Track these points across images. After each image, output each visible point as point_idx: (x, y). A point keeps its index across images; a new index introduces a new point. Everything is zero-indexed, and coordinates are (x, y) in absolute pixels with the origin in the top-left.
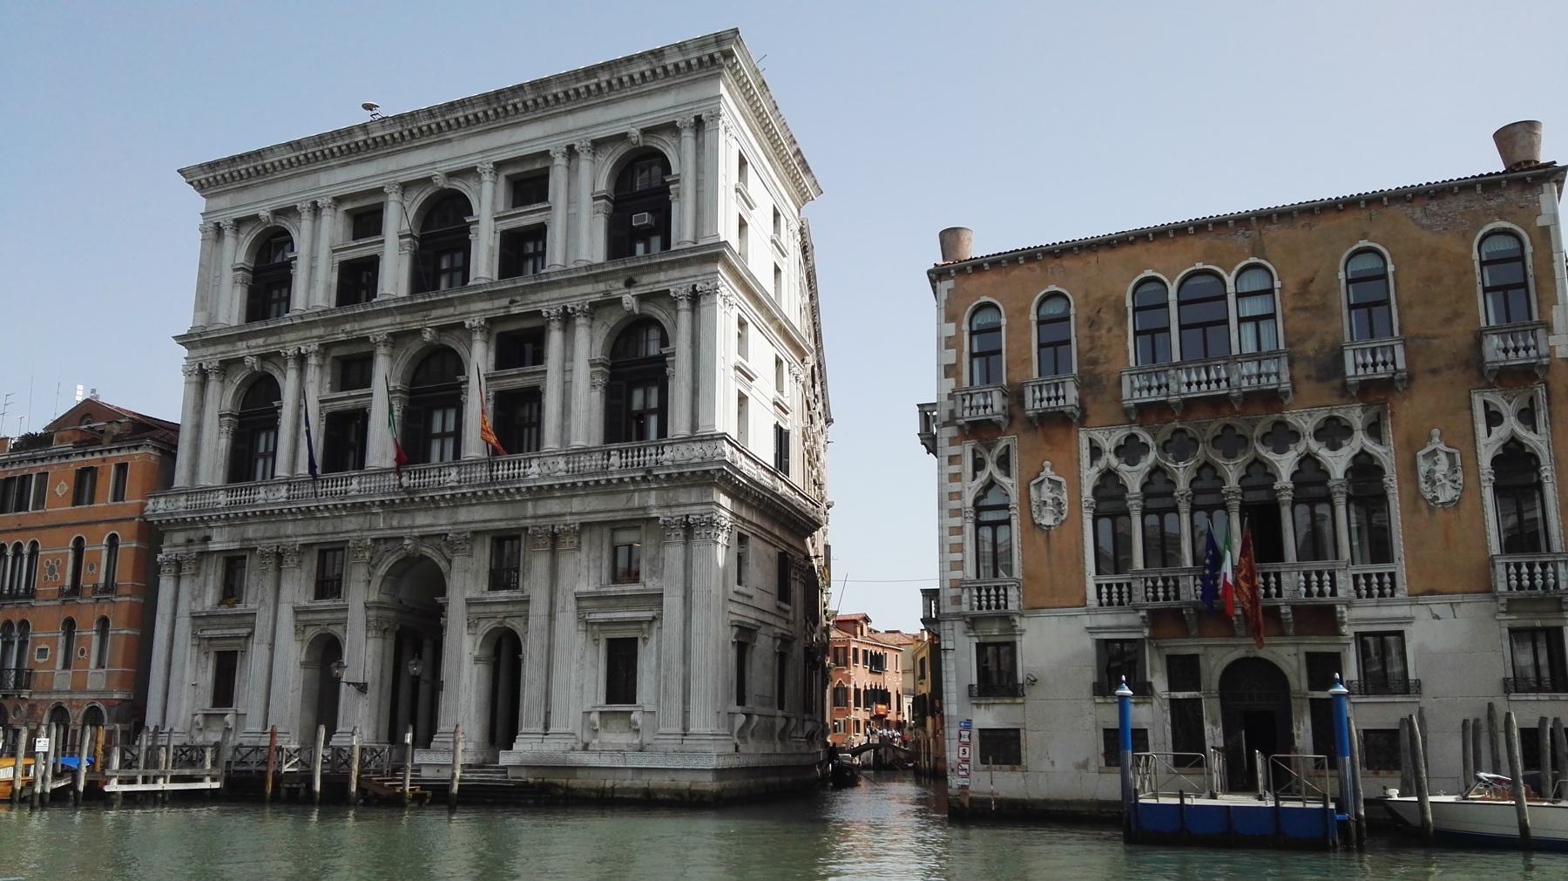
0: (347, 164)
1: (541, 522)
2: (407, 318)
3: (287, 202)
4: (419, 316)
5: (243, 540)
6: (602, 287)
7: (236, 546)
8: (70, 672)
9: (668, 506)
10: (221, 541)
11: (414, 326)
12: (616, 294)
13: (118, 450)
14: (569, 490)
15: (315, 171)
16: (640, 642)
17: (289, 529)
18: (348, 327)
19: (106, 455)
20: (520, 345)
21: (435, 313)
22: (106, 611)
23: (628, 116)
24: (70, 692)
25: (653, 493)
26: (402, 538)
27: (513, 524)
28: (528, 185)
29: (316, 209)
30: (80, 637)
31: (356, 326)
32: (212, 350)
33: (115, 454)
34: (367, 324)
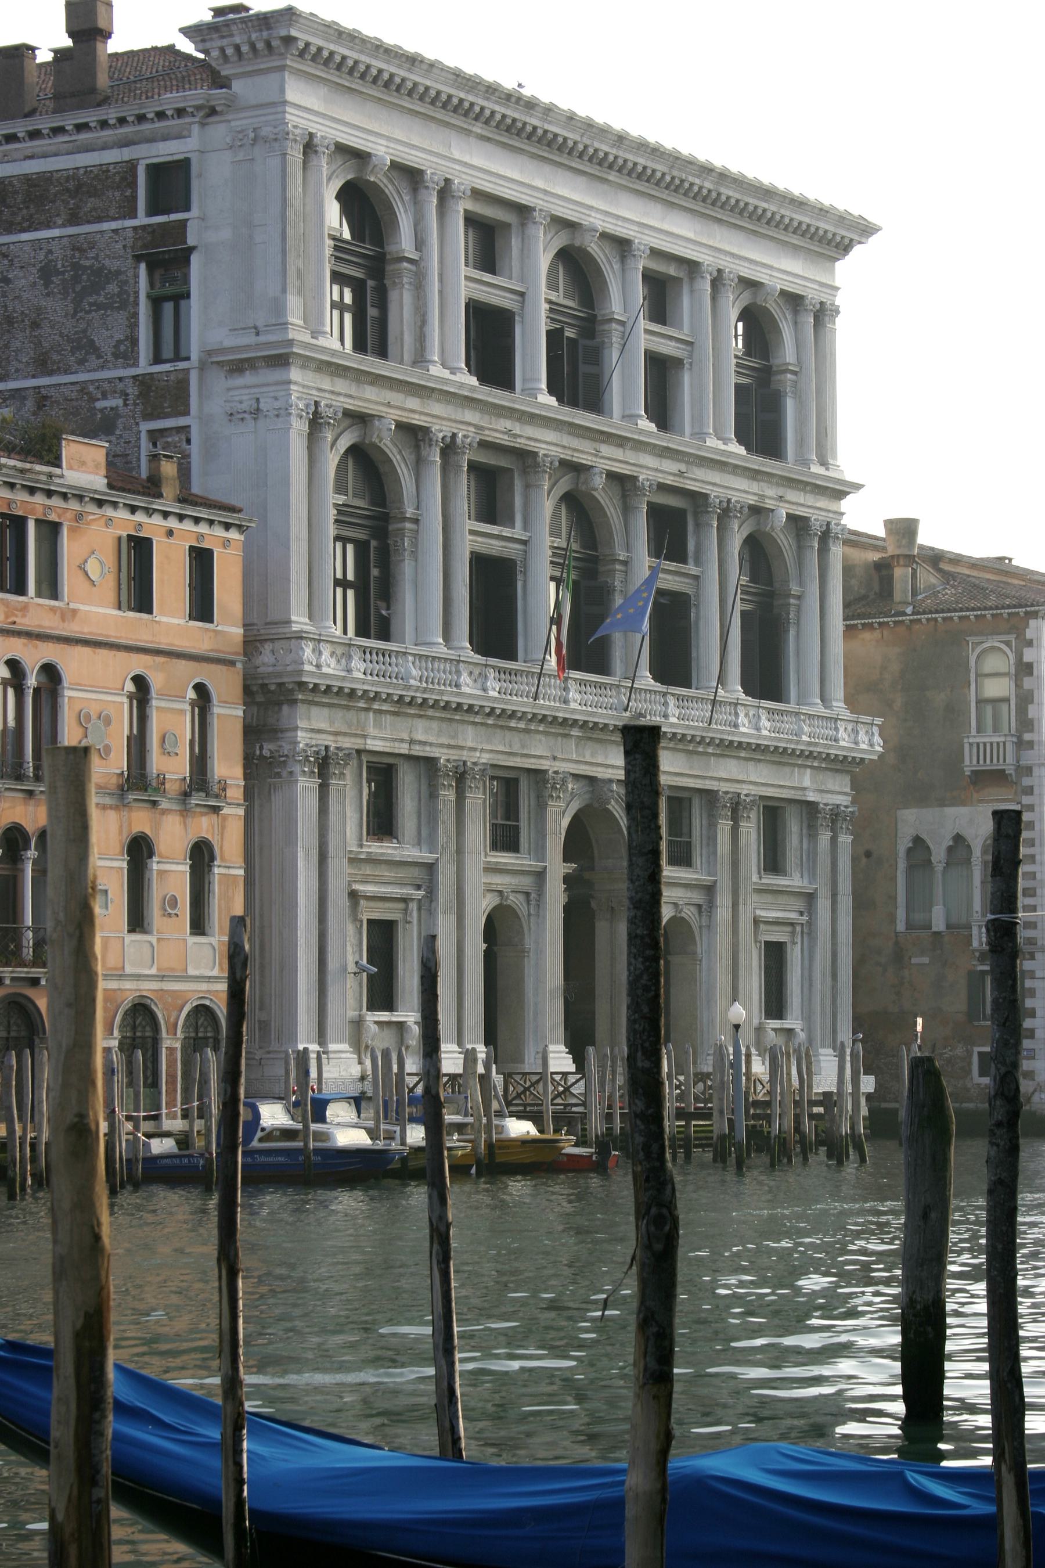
0: (488, 139)
1: (724, 787)
2: (575, 443)
3: (413, 158)
4: (586, 445)
5: (412, 742)
6: (755, 487)
7: (404, 749)
8: (153, 940)
9: (822, 791)
10: (382, 737)
11: (585, 459)
12: (769, 504)
13: (197, 520)
14: (757, 752)
15: (447, 125)
16: (789, 945)
17: (469, 736)
18: (506, 424)
19: (172, 523)
20: (673, 527)
21: (606, 450)
22: (204, 826)
23: (780, 268)
24: (162, 978)
25: (808, 771)
26: (591, 780)
27: (699, 784)
28: (661, 295)
29: (445, 193)
30: (161, 873)
31: (517, 429)
32: (326, 383)
33: (188, 525)
34: (530, 431)
